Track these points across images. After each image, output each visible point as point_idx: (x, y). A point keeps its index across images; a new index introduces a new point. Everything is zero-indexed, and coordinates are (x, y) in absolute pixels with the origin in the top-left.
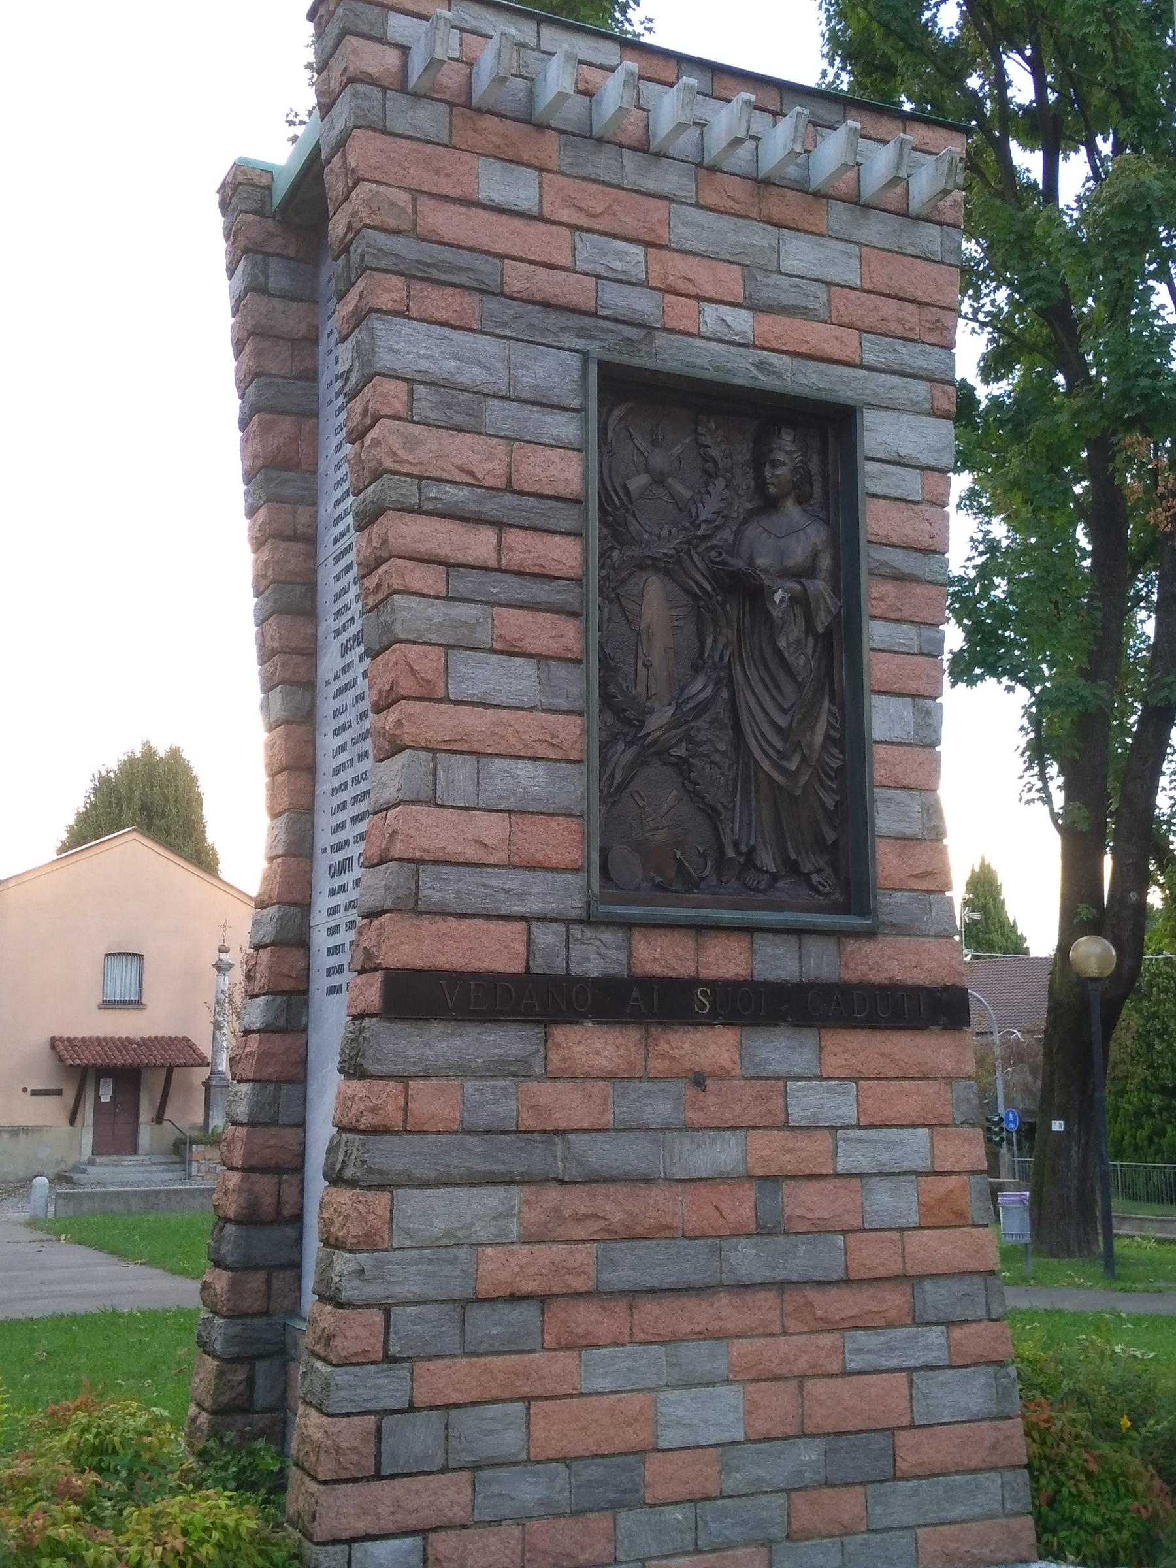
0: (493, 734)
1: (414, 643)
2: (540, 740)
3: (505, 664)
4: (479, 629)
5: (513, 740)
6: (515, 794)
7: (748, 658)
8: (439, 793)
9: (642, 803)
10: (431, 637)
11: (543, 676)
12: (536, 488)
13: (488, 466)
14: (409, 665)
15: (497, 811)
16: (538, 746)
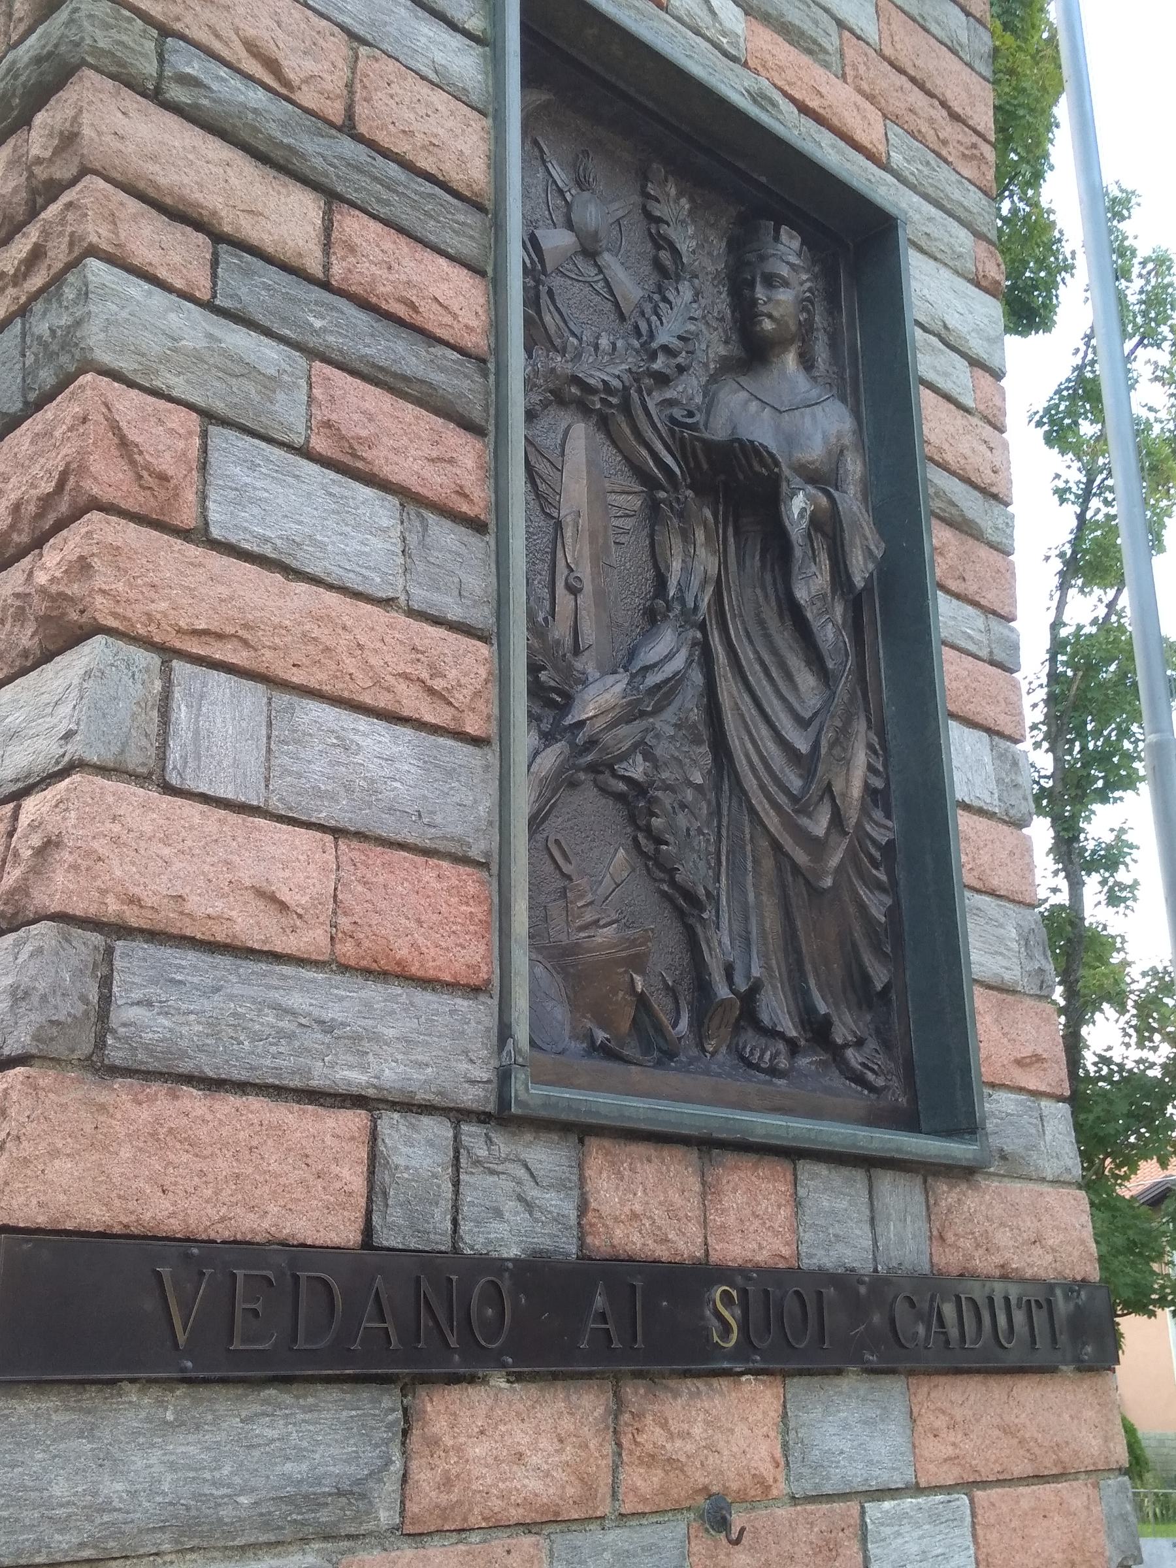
0: (306, 638)
1: (131, 384)
2: (405, 676)
3: (335, 489)
4: (280, 396)
5: (350, 665)
6: (349, 789)
7: (734, 616)
8: (174, 755)
9: (566, 868)
10: (173, 380)
11: (412, 539)
12: (402, 147)
13: (310, 66)
14: (115, 428)
15: (308, 825)
16: (402, 687)
